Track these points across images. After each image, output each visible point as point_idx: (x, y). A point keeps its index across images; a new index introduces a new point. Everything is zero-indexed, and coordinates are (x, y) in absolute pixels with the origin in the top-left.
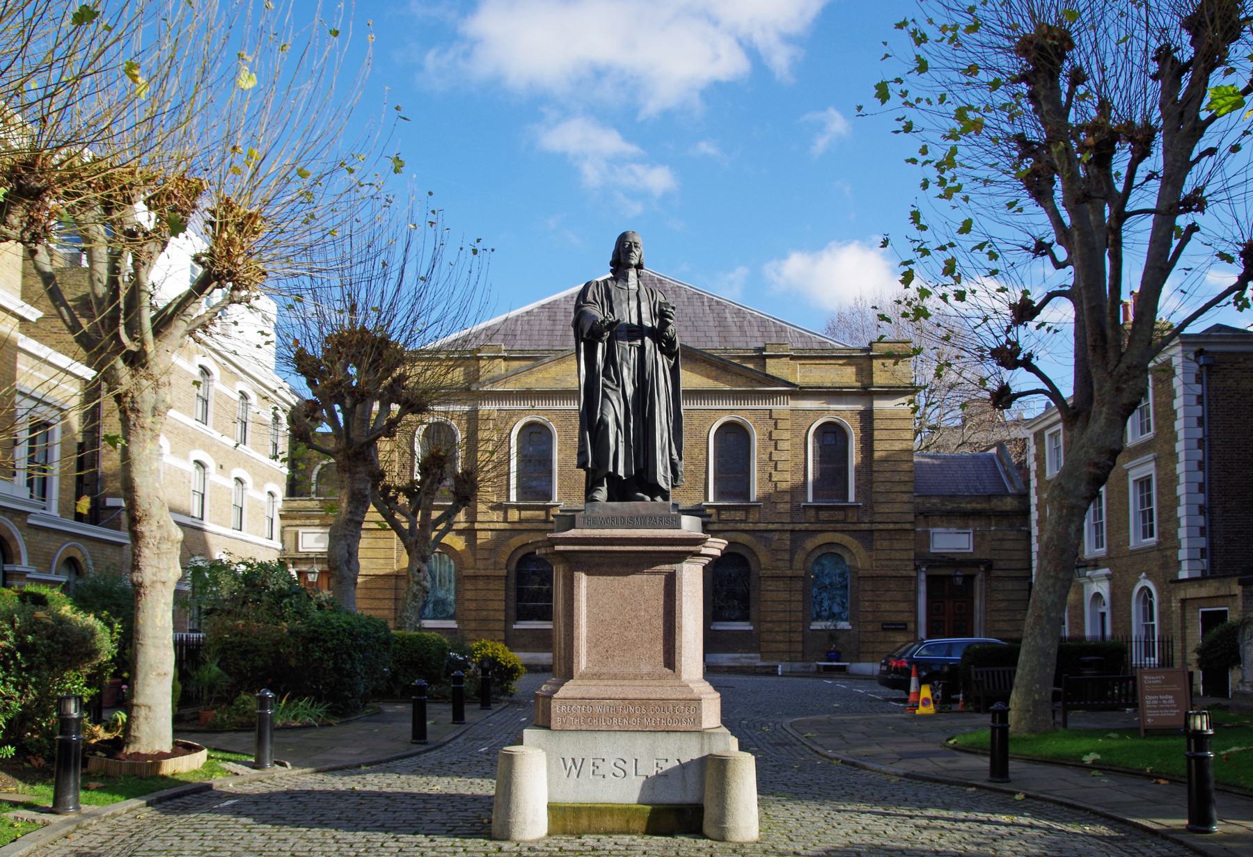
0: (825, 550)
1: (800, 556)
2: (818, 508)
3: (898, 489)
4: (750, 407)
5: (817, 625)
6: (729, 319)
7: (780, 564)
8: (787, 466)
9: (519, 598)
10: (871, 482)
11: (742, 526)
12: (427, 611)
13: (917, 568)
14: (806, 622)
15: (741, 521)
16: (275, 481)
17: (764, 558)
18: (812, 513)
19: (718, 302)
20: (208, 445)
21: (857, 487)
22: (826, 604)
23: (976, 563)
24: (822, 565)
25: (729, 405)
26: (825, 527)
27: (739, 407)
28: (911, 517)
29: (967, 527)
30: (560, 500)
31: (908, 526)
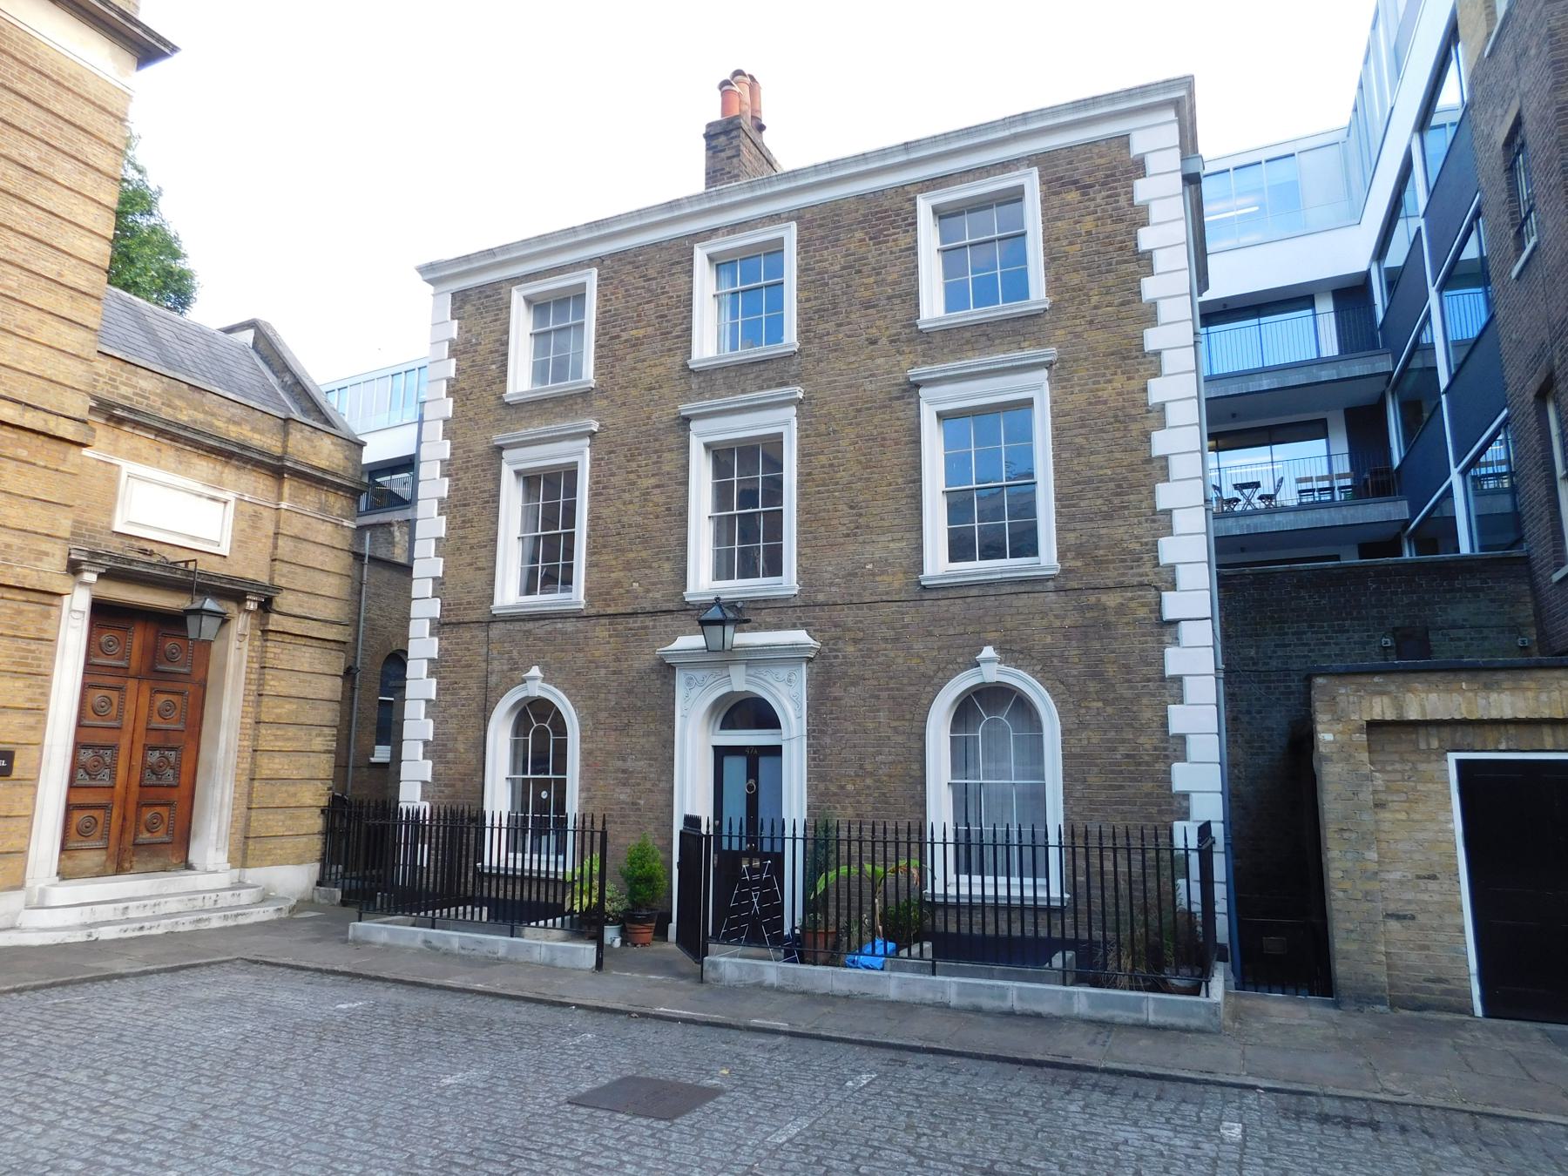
13: (74, 568)
23: (233, 591)
28: (79, 405)
29: (219, 484)
31: (67, 430)
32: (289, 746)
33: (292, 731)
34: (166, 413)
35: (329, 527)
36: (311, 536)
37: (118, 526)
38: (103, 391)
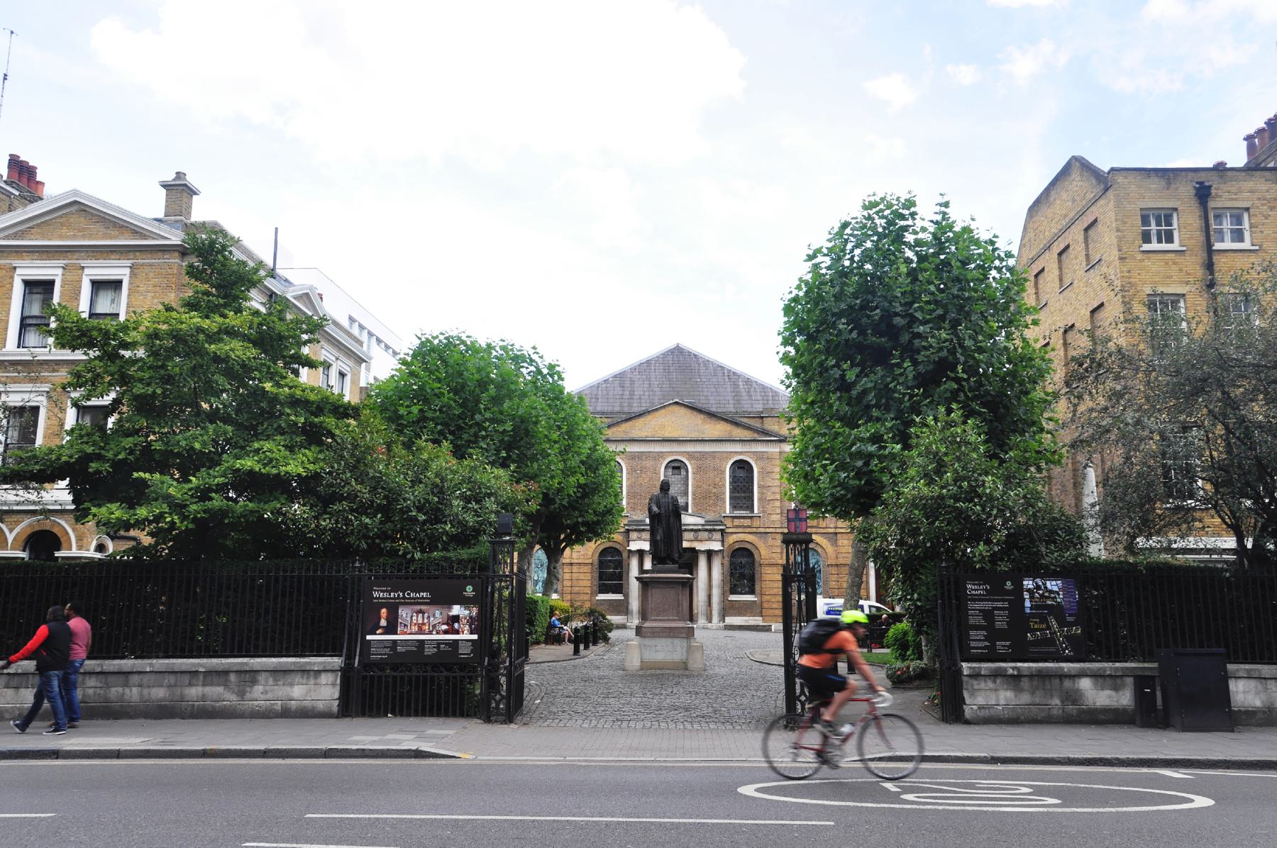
8: (777, 490)
9: (601, 578)
25: (738, 448)
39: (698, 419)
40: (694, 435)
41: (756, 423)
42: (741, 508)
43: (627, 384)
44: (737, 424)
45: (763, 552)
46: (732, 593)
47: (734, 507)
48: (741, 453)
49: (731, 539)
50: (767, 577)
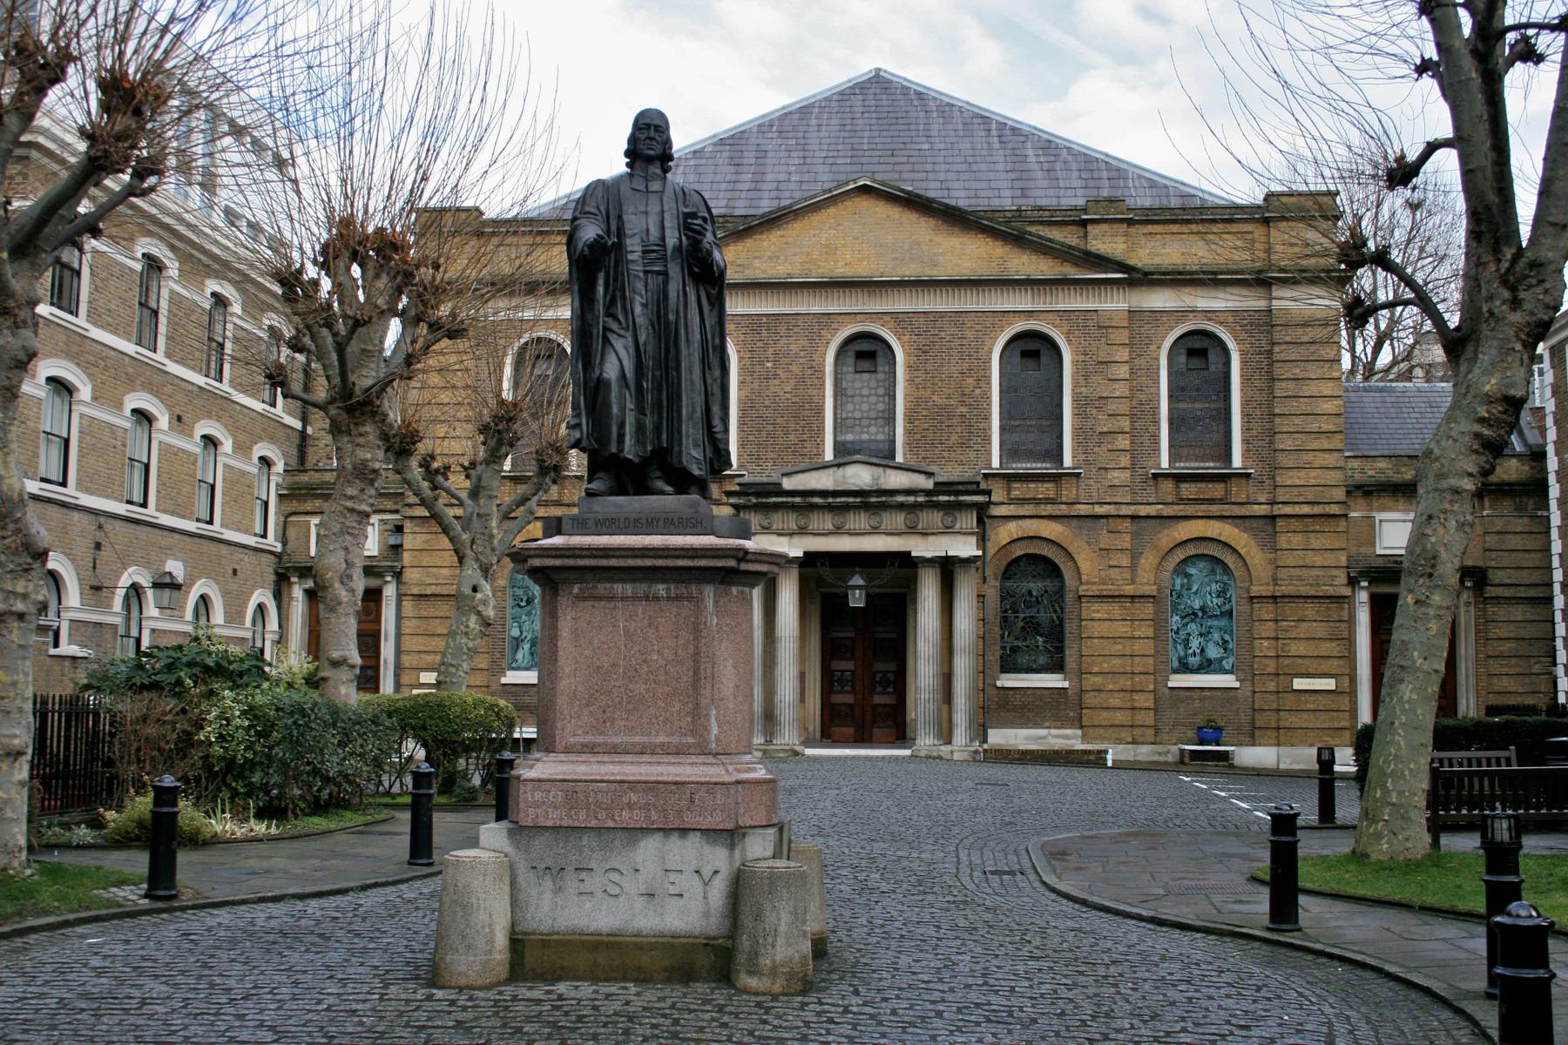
0: (1191, 550)
1: (1148, 561)
2: (1179, 478)
3: (1316, 445)
4: (1061, 307)
5: (1178, 681)
6: (1032, 159)
7: (1115, 573)
8: (1124, 407)
10: (1272, 433)
11: (1048, 509)
12: (519, 656)
13: (1352, 582)
14: (1160, 674)
15: (1048, 501)
16: (272, 439)
17: (1087, 562)
18: (1168, 486)
19: (1013, 129)
20: (157, 382)
21: (1245, 441)
22: (1195, 644)
24: (1188, 576)
26: (1190, 510)
27: (1041, 307)
28: (1340, 494)
30: (741, 466)
31: (1335, 509)
32: (1513, 671)
33: (1513, 661)
34: (1397, 478)
35: (1526, 520)
36: (1509, 528)
37: (1379, 552)
38: (1358, 478)
39: (922, 229)
40: (910, 271)
41: (1066, 236)
42: (1031, 455)
43: (749, 157)
44: (1018, 240)
45: (1085, 566)
46: (1008, 667)
47: (1009, 453)
48: (1030, 314)
49: (1004, 533)
50: (1095, 629)
